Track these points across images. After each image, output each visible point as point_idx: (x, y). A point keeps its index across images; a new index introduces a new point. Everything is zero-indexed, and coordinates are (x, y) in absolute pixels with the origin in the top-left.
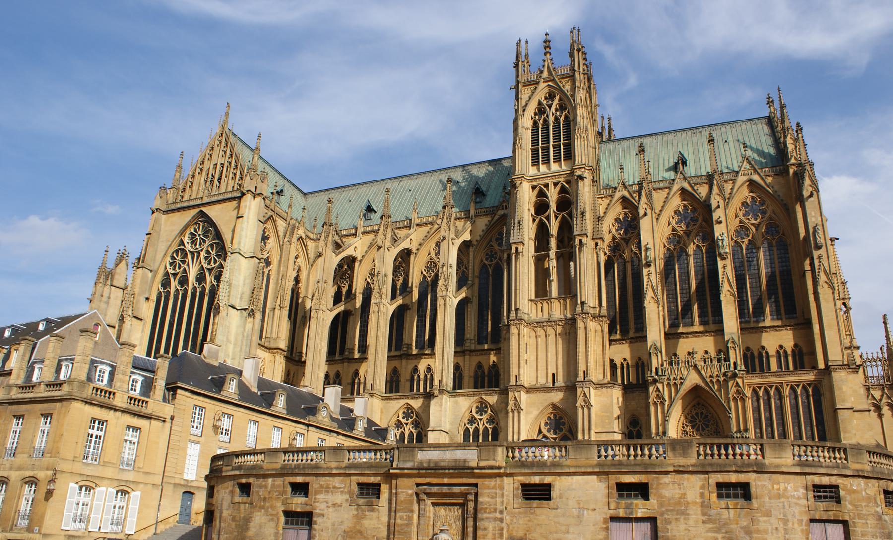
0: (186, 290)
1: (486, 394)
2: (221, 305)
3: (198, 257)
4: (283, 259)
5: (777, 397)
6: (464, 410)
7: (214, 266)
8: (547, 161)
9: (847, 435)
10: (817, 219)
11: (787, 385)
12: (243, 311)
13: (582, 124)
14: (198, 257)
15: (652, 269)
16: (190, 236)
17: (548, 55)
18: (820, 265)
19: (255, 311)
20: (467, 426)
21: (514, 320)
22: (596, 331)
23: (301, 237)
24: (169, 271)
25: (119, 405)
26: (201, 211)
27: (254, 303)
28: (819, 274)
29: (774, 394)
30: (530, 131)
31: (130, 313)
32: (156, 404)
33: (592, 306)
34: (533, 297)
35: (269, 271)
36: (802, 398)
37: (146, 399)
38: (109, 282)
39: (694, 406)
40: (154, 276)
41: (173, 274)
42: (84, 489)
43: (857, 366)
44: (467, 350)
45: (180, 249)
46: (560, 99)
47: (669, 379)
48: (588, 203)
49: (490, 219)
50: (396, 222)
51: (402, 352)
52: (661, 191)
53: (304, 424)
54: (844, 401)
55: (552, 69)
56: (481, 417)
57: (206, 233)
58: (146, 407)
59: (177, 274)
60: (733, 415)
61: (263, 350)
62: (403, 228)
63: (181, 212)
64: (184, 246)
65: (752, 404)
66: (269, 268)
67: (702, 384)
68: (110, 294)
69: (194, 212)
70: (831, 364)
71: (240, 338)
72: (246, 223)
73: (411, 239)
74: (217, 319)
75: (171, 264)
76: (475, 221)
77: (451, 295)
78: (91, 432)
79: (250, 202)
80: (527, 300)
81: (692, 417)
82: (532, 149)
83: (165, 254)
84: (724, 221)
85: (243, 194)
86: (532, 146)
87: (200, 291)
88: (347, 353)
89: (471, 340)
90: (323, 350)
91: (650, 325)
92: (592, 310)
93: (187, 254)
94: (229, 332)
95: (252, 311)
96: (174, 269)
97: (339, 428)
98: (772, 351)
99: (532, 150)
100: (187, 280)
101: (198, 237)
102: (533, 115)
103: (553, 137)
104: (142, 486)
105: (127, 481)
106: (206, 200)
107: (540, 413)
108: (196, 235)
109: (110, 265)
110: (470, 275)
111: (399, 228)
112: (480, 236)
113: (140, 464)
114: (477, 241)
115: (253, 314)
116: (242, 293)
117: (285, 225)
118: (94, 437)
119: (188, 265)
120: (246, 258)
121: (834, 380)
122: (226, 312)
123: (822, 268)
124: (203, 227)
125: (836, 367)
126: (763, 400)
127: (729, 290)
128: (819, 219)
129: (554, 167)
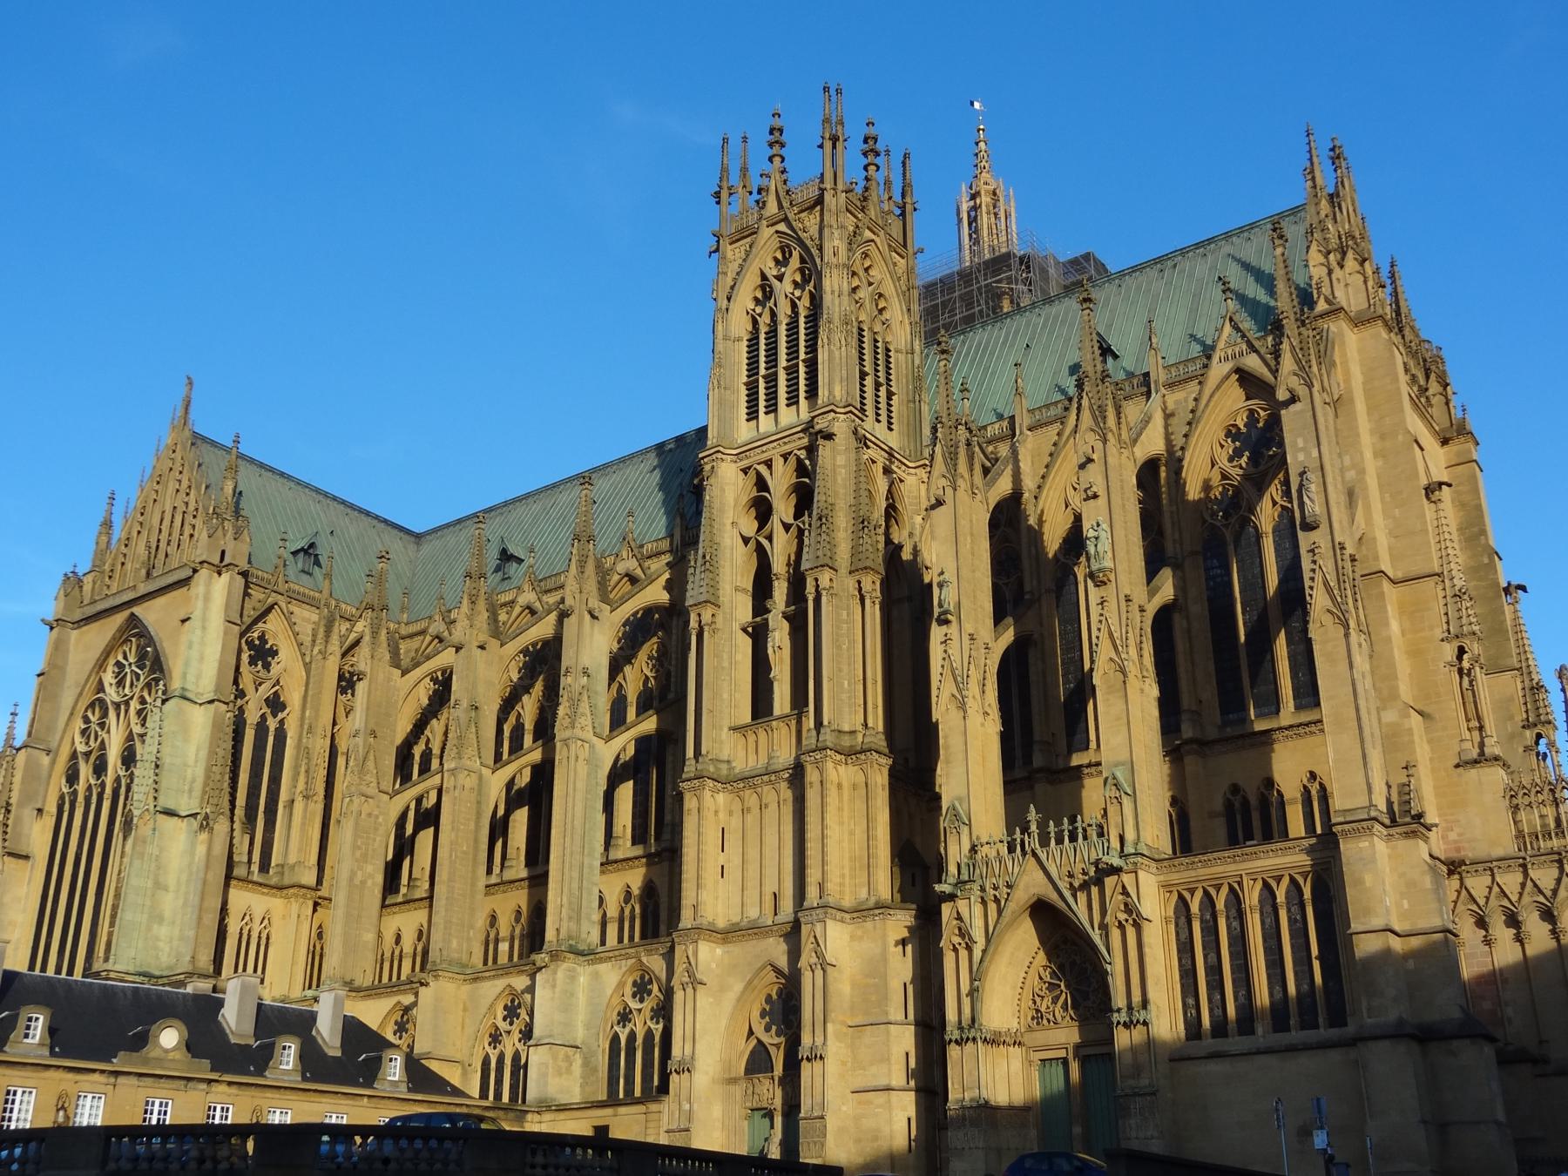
0: (103, 785)
2: (136, 813)
3: (126, 711)
4: (310, 693)
5: (1233, 912)
6: (609, 992)
8: (772, 408)
10: (1308, 454)
11: (1255, 880)
12: (192, 819)
13: (837, 309)
14: (127, 711)
15: (953, 630)
16: (117, 670)
17: (777, 160)
18: (1313, 571)
19: (211, 816)
20: (615, 1028)
22: (855, 787)
26: (132, 614)
28: (1314, 593)
29: (1226, 906)
30: (746, 343)
33: (846, 728)
34: (746, 716)
36: (1289, 911)
40: (53, 762)
43: (1413, 817)
45: (98, 699)
46: (802, 260)
47: (983, 889)
48: (842, 491)
50: (545, 578)
52: (1044, 430)
53: (103, 1072)
54: (1367, 912)
55: (782, 194)
56: (639, 1006)
57: (142, 657)
59: (91, 752)
61: (263, 893)
63: (102, 621)
64: (104, 692)
65: (1177, 934)
66: (280, 716)
67: (1054, 897)
69: (120, 618)
70: (1341, 819)
71: (184, 877)
72: (198, 632)
74: (130, 841)
75: (84, 732)
77: (589, 735)
79: (209, 584)
80: (726, 730)
82: (746, 384)
83: (72, 714)
84: (1102, 492)
85: (195, 571)
86: (748, 376)
90: (369, 882)
91: (948, 762)
92: (847, 737)
93: (107, 708)
94: (159, 868)
97: (212, 1070)
100: (106, 762)
101: (127, 670)
102: (751, 305)
106: (143, 589)
107: (746, 988)
108: (124, 665)
111: (549, 591)
115: (208, 824)
116: (194, 781)
117: (315, 617)
119: (108, 732)
120: (201, 704)
121: (1344, 860)
122: (151, 825)
123: (1319, 577)
124: (138, 646)
125: (1346, 827)
126: (1202, 922)
127: (1111, 659)
128: (1315, 453)
129: (787, 416)
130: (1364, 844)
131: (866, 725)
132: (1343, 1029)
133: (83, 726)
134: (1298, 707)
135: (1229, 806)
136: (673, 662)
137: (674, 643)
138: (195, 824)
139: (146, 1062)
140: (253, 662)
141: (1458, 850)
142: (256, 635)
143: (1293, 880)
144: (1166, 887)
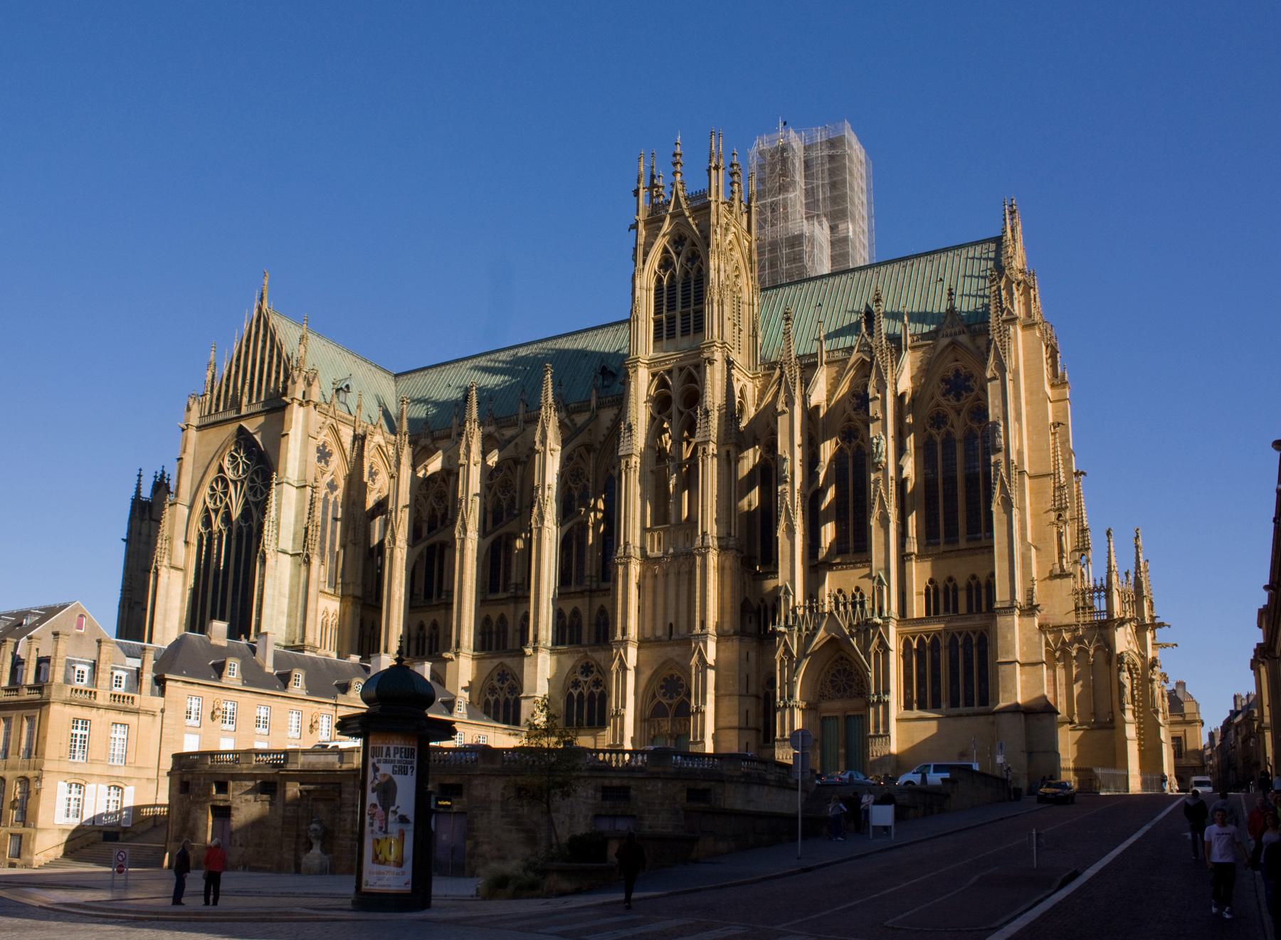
1: (592, 651)
2: (267, 551)
7: (260, 498)
9: (1006, 695)
21: (621, 558)
23: (379, 446)
24: (209, 506)
25: (102, 703)
27: (310, 546)
31: (166, 562)
32: (146, 698)
35: (336, 498)
36: (964, 649)
37: (131, 695)
38: (147, 516)
39: (837, 661)
41: (214, 510)
42: (74, 785)
44: (585, 590)
49: (615, 411)
51: (509, 595)
58: (133, 703)
60: (872, 674)
62: (508, 426)
64: (224, 472)
66: (336, 493)
68: (150, 531)
69: (233, 428)
73: (516, 444)
75: (212, 496)
76: (597, 416)
78: (74, 731)
81: (833, 675)
87: (247, 532)
88: (443, 597)
89: (591, 577)
94: (280, 584)
95: (308, 556)
96: (215, 503)
98: (962, 583)
99: (655, 321)
101: (239, 459)
102: (657, 268)
103: (682, 299)
104: (135, 781)
105: (118, 777)
109: (146, 493)
110: (590, 491)
111: (504, 427)
112: (604, 435)
113: (131, 759)
114: (600, 442)
116: (295, 534)
118: (79, 736)
119: (230, 498)
122: (274, 560)
130: (1009, 619)
131: (729, 534)
132: (987, 707)
133: (211, 493)
134: (968, 540)
135: (927, 589)
136: (591, 480)
137: (591, 469)
138: (299, 560)
139: (349, 699)
140: (319, 461)
141: (1046, 619)
142: (321, 443)
143: (968, 634)
144: (900, 634)
